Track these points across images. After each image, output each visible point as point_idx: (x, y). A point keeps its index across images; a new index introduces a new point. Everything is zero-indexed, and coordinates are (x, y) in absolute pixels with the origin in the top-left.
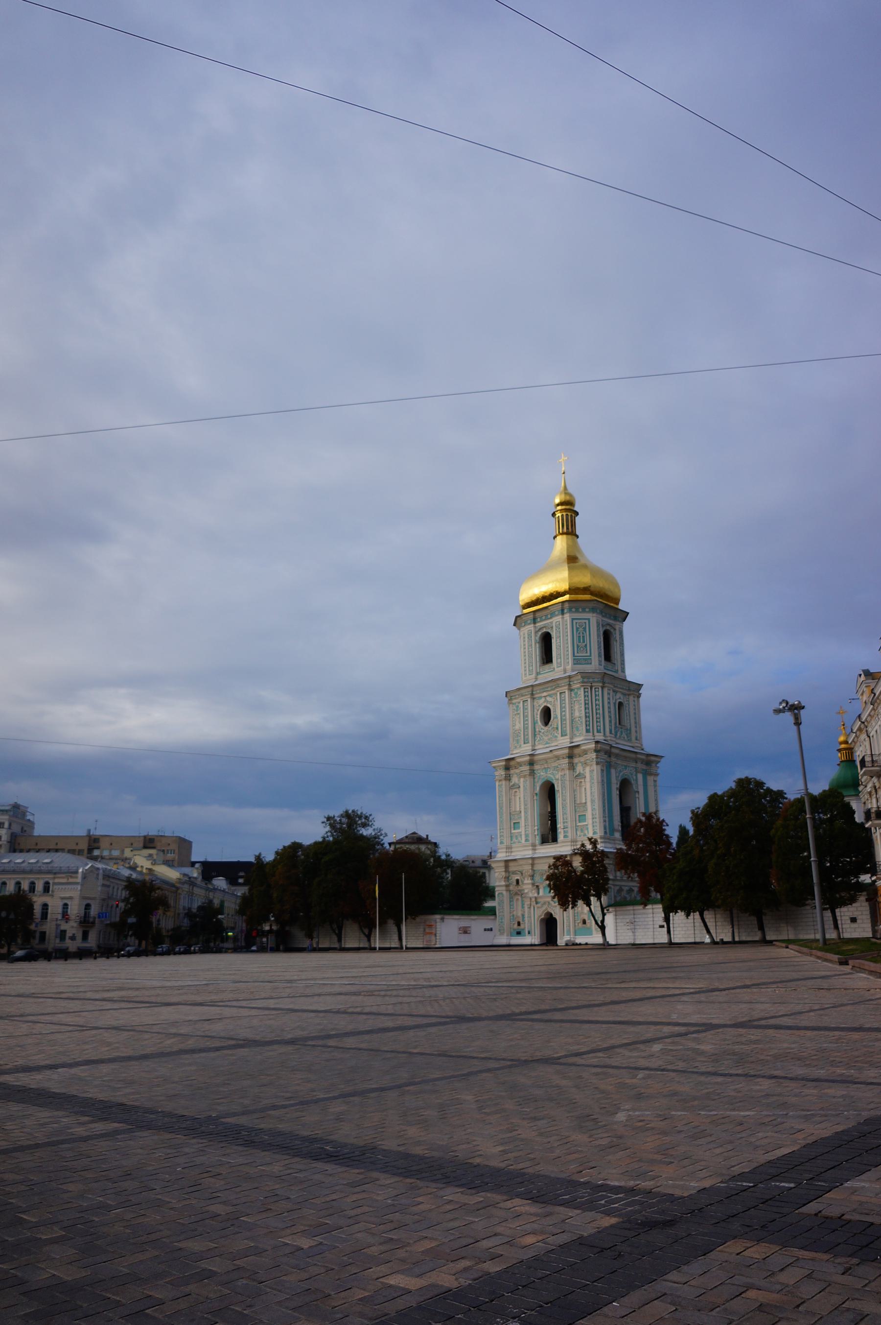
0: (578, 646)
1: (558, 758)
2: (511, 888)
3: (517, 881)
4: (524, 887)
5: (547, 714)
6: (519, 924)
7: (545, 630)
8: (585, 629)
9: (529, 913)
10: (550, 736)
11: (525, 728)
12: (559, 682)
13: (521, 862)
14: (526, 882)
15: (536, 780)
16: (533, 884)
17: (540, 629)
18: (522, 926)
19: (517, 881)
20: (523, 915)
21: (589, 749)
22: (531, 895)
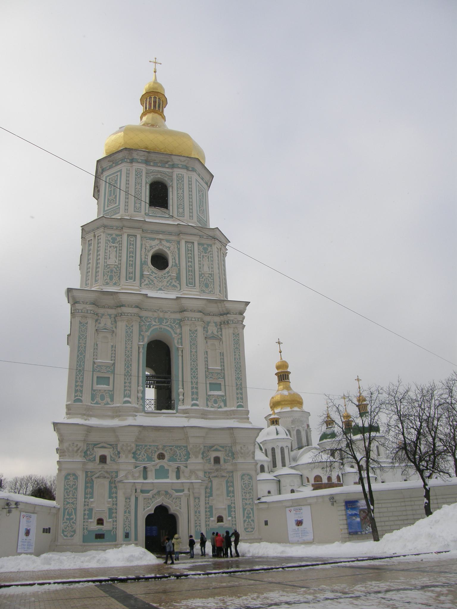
0: (200, 208)
3: (103, 459)
6: (100, 522)
7: (159, 176)
8: (203, 194)
10: (165, 283)
11: (131, 264)
14: (123, 459)
15: (144, 328)
18: (107, 526)
19: (103, 459)
20: (112, 512)
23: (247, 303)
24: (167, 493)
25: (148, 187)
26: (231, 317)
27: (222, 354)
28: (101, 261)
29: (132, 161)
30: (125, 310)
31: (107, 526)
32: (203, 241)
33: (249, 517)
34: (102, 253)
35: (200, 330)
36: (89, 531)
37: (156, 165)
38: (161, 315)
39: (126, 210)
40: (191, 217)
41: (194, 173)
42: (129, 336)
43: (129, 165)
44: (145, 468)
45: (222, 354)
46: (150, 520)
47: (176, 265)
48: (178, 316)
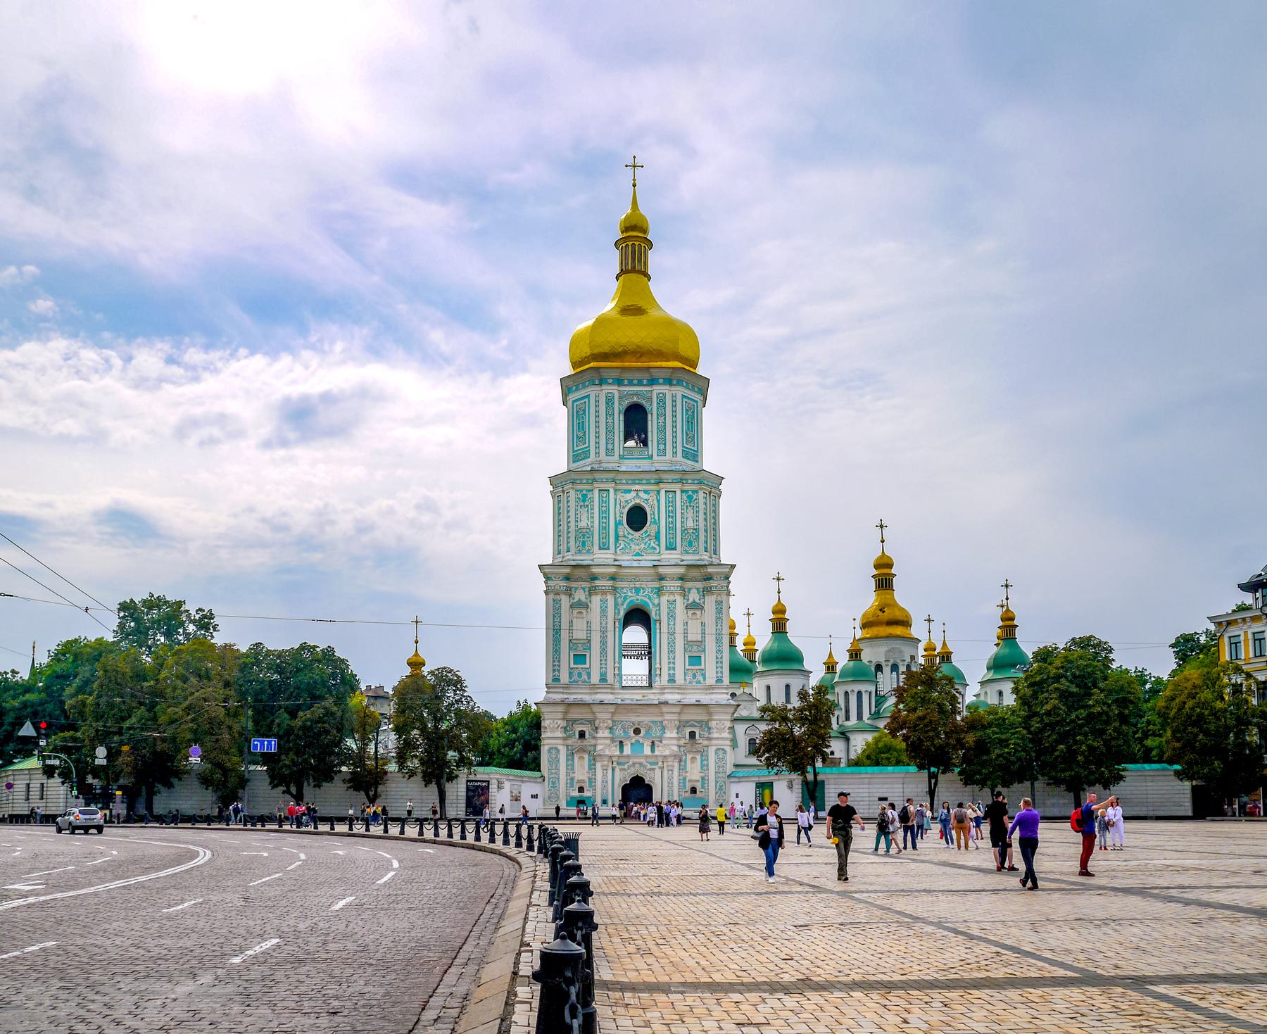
1: (661, 578)
2: (569, 742)
3: (582, 735)
4: (593, 742)
5: (637, 518)
6: (581, 790)
9: (605, 776)
11: (604, 528)
12: (664, 476)
13: (595, 708)
14: (600, 734)
15: (620, 600)
16: (612, 740)
17: (629, 395)
18: (587, 794)
19: (582, 735)
20: (592, 781)
21: (718, 573)
22: (607, 752)
23: (733, 566)
24: (641, 764)
25: (622, 418)
26: (713, 583)
27: (703, 624)
28: (572, 524)
29: (602, 382)
30: (598, 583)
31: (587, 794)
32: (687, 487)
33: (721, 788)
34: (572, 514)
35: (679, 599)
36: (572, 798)
37: (631, 384)
38: (638, 585)
39: (597, 454)
40: (675, 453)
41: (679, 388)
42: (604, 611)
43: (598, 388)
44: (621, 742)
45: (703, 624)
46: (625, 789)
47: (655, 523)
48: (656, 585)
